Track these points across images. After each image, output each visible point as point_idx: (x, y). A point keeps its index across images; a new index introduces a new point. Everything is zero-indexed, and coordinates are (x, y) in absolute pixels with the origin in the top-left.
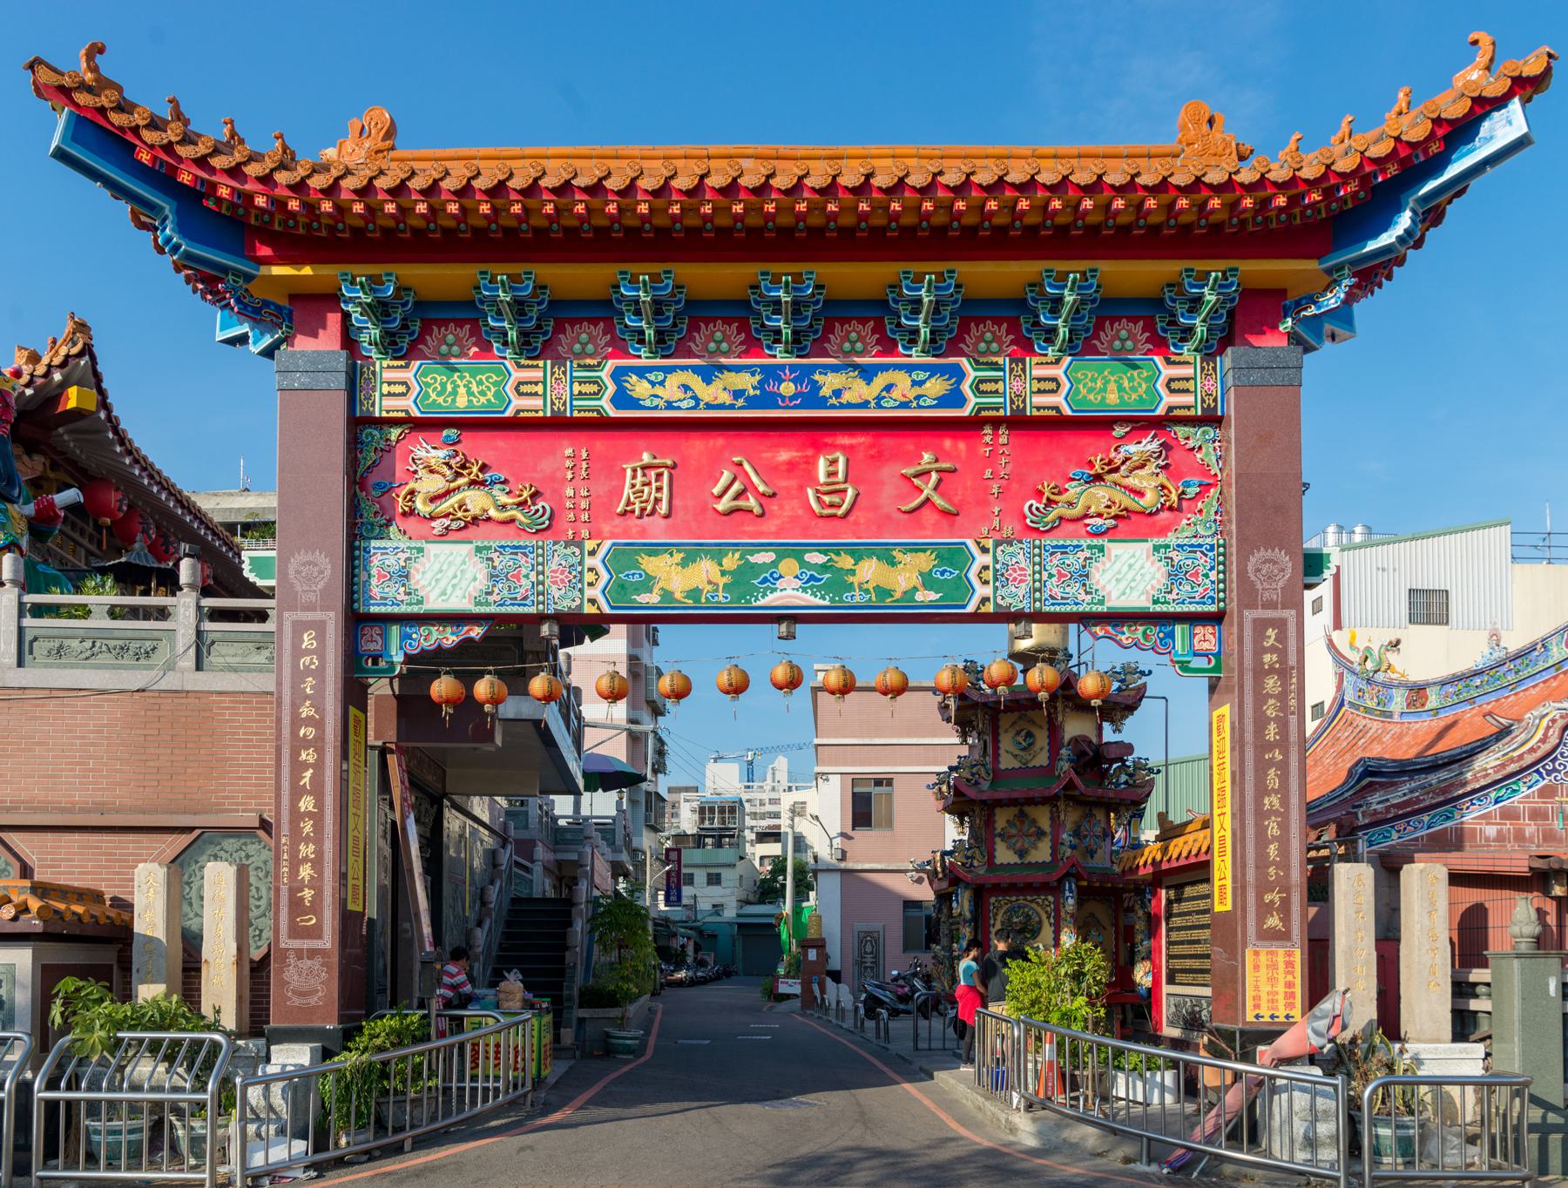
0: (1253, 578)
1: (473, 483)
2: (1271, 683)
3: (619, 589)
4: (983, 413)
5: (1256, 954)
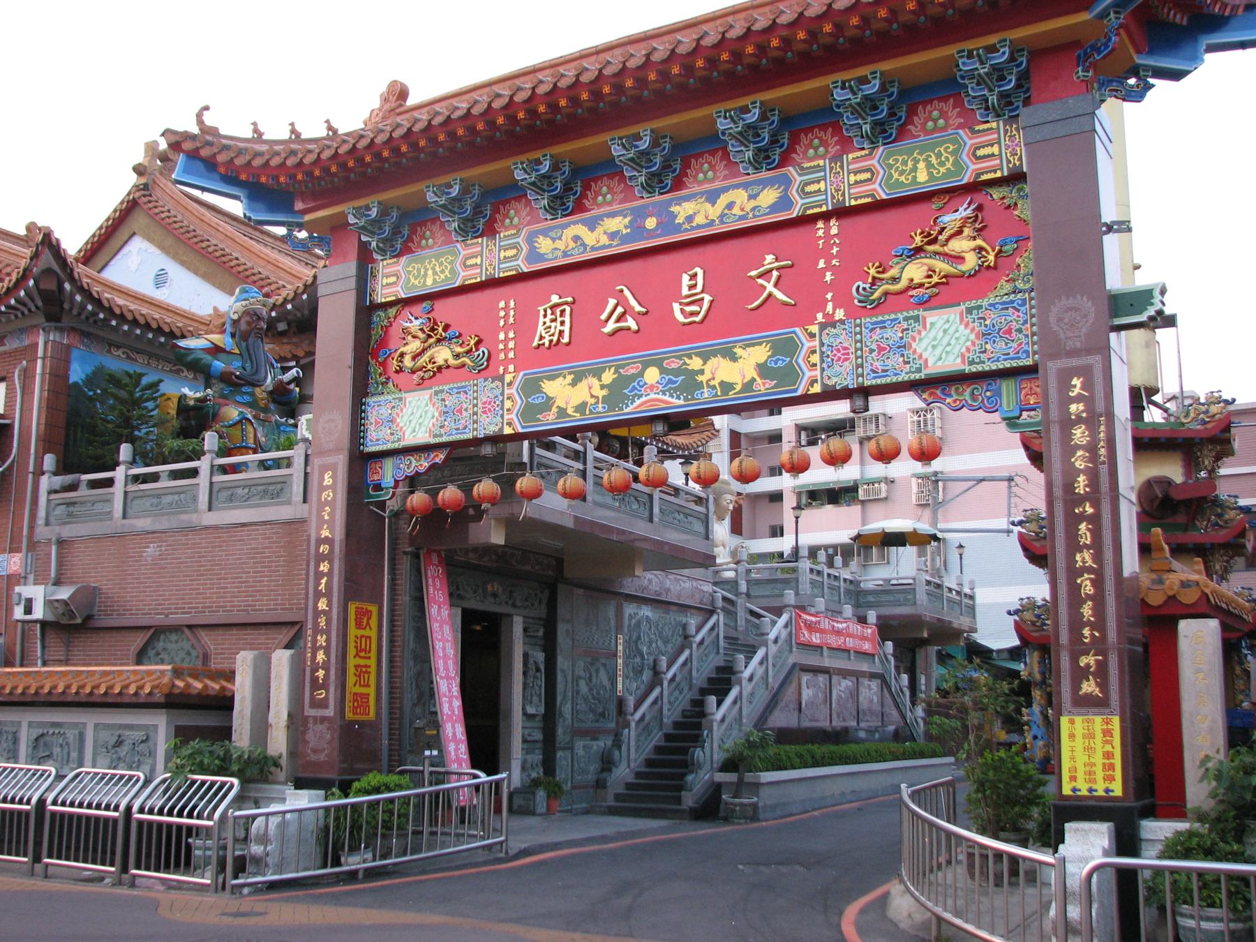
0: (1055, 328)
1: (439, 341)
2: (1080, 434)
3: (529, 412)
4: (809, 212)
5: (1072, 722)
